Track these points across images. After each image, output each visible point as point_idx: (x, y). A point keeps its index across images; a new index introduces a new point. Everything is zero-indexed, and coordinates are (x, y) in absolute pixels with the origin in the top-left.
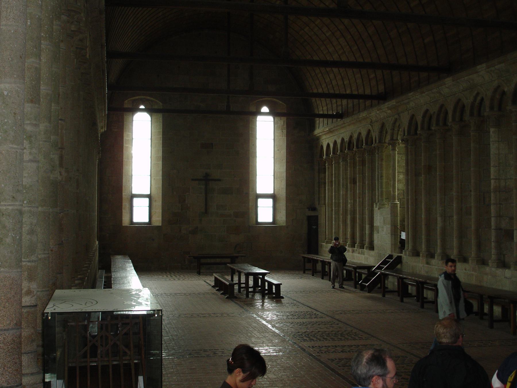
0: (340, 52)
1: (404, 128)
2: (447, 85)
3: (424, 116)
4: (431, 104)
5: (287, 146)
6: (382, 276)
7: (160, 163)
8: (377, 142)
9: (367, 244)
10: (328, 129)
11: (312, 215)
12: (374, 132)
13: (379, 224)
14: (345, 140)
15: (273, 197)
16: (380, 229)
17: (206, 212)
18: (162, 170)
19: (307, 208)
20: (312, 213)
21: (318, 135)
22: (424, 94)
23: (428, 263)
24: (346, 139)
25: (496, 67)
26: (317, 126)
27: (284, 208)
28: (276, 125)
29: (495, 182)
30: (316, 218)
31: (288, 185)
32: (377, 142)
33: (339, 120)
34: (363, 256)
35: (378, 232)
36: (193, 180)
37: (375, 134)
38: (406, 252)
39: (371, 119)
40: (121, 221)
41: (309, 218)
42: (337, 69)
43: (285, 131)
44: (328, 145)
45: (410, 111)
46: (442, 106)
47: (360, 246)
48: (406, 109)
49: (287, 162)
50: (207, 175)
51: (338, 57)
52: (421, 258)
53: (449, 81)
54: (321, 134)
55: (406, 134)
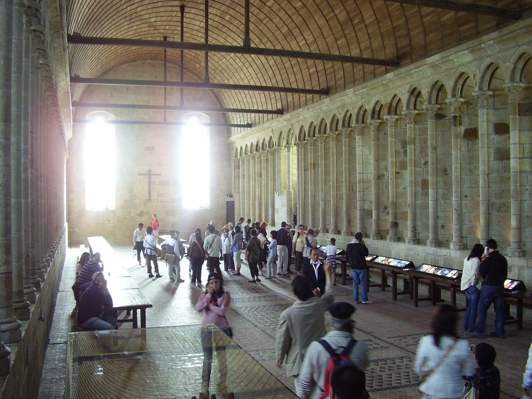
2: (326, 104)
3: (310, 127)
8: (277, 145)
14: (254, 144)
16: (279, 211)
17: (150, 199)
20: (230, 199)
21: (234, 140)
22: (309, 110)
24: (255, 144)
25: (360, 91)
26: (233, 133)
29: (360, 175)
32: (277, 145)
33: (249, 128)
35: (278, 213)
36: (139, 175)
37: (275, 140)
41: (228, 203)
42: (247, 91)
44: (241, 148)
46: (323, 119)
50: (150, 171)
53: (327, 101)
55: (297, 140)
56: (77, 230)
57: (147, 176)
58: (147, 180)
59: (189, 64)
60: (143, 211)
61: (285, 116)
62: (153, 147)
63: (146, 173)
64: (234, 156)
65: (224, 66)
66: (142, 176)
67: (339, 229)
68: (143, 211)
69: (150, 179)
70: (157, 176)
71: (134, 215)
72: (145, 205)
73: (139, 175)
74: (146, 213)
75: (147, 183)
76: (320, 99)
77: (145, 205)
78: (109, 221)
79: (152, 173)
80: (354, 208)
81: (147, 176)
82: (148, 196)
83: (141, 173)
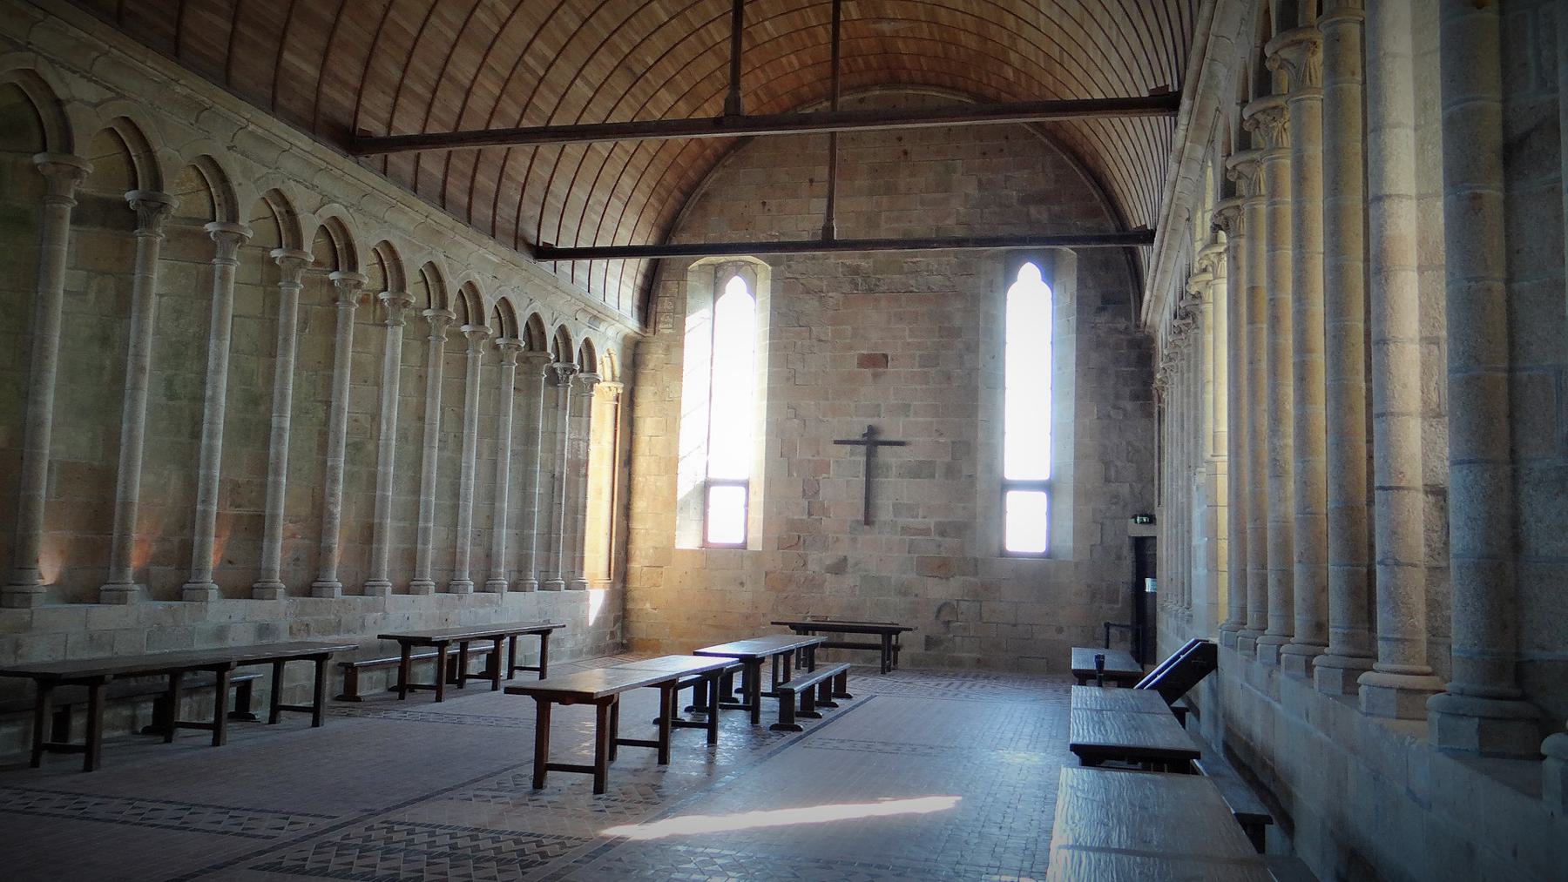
5: (1078, 358)
7: (764, 403)
15: (1049, 487)
17: (868, 520)
18: (767, 422)
19: (1133, 518)
20: (1144, 531)
27: (1071, 515)
28: (1055, 307)
31: (1079, 457)
36: (836, 442)
40: (671, 539)
42: (1154, 117)
43: (1073, 319)
49: (1079, 398)
57: (863, 448)
58: (863, 459)
60: (845, 559)
62: (886, 356)
63: (857, 438)
66: (848, 447)
68: (845, 559)
69: (870, 455)
70: (895, 448)
71: (817, 569)
72: (854, 540)
73: (836, 442)
74: (856, 564)
75: (862, 469)
77: (854, 540)
78: (742, 584)
79: (882, 438)
81: (863, 448)
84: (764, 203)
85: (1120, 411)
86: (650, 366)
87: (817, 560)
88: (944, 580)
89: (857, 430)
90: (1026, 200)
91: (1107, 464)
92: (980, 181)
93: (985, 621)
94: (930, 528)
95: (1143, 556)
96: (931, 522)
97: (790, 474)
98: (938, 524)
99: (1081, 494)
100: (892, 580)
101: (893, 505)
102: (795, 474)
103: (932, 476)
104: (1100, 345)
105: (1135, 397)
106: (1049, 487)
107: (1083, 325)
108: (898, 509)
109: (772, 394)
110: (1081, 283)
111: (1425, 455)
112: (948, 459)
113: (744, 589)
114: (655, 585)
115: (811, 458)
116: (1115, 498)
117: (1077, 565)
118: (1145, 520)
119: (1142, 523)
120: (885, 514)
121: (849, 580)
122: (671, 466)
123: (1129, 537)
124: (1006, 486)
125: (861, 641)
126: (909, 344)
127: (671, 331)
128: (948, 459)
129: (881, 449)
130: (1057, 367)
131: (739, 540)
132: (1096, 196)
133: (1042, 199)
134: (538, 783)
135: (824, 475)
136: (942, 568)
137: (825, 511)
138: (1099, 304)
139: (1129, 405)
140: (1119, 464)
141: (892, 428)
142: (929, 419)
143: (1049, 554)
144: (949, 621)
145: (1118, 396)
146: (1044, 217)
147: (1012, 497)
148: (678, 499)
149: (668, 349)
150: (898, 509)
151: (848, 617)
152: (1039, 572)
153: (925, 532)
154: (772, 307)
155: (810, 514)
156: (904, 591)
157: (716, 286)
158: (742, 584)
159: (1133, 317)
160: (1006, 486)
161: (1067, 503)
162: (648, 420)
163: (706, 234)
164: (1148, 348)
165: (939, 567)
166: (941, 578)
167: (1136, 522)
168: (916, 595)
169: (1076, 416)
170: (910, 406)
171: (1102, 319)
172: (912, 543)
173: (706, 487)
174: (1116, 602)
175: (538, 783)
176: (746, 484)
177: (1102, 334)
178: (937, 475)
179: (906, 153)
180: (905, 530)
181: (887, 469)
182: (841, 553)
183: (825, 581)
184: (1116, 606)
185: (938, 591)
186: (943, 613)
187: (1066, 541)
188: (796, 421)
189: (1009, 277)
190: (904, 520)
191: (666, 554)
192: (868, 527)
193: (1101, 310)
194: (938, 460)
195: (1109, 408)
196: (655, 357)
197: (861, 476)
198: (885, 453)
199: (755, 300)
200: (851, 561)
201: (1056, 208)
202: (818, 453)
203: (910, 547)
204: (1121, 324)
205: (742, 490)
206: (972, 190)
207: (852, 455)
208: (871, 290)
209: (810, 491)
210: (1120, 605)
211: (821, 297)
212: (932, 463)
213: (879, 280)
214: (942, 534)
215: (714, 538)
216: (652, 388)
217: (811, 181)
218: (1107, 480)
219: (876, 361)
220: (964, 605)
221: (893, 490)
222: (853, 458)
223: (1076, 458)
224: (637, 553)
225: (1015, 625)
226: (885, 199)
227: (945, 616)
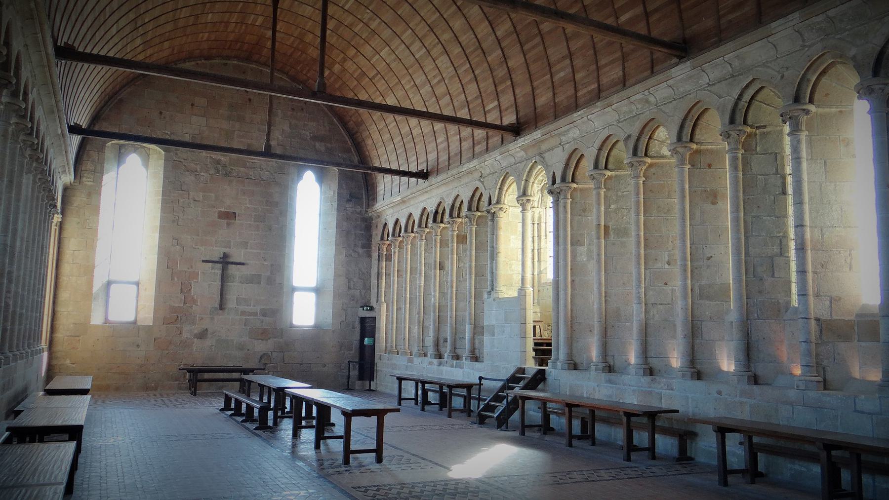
0: (434, 82)
1: (554, 173)
2: (671, 82)
4: (619, 125)
6: (520, 401)
7: (157, 235)
9: (465, 353)
10: (400, 198)
11: (367, 316)
12: (486, 189)
13: (494, 322)
15: (318, 291)
17: (222, 307)
19: (361, 307)
23: (610, 381)
28: (322, 197)
30: (374, 318)
31: (336, 275)
34: (461, 371)
36: (204, 261)
38: (554, 363)
39: (481, 172)
40: (88, 318)
41: (363, 320)
43: (335, 204)
45: (567, 146)
47: (452, 356)
48: (560, 144)
49: (337, 245)
50: (225, 256)
51: (431, 89)
52: (593, 373)
54: (384, 208)
56: (68, 362)
57: (220, 265)
58: (219, 272)
59: (308, 71)
61: (528, 137)
62: (235, 213)
63: (216, 259)
64: (379, 237)
65: (381, 67)
66: (210, 264)
67: (698, 367)
69: (224, 270)
72: (212, 319)
73: (204, 261)
75: (219, 277)
76: (652, 72)
78: (138, 346)
79: (231, 260)
80: (758, 318)
82: (218, 301)
83: (207, 259)
84: (161, 113)
85: (357, 253)
86: (75, 205)
87: (188, 331)
88: (264, 341)
89: (217, 253)
90: (315, 138)
91: (349, 280)
92: (290, 124)
93: (286, 362)
94: (257, 312)
95: (367, 327)
96: (258, 309)
97: (173, 279)
98: (261, 310)
99: (337, 295)
100: (235, 342)
101: (237, 299)
102: (176, 279)
103: (259, 283)
104: (348, 219)
105: (363, 247)
106: (317, 290)
107: (340, 208)
108: (239, 301)
109: (163, 229)
110: (340, 186)
111: (814, 307)
112: (268, 274)
113: (139, 349)
114: (73, 348)
115: (186, 269)
116: (353, 298)
117: (333, 331)
118: (368, 308)
119: (367, 310)
120: (231, 304)
121: (209, 342)
122: (89, 271)
123: (359, 317)
124: (294, 289)
125: (215, 377)
126: (248, 208)
127: (92, 183)
128: (268, 274)
129: (231, 267)
130: (324, 228)
131: (131, 318)
132: (349, 142)
133: (321, 139)
134: (346, 461)
135: (194, 280)
136: (264, 334)
137: (194, 301)
138: (348, 197)
139: (361, 251)
140: (355, 280)
141: (237, 255)
142: (259, 251)
143: (316, 326)
144: (266, 364)
145: (355, 246)
146: (323, 149)
147: (297, 296)
148: (93, 292)
149: (89, 195)
150: (239, 301)
151: (208, 364)
152: (316, 334)
153: (255, 314)
154: (165, 177)
155: (185, 303)
156: (241, 347)
157: (120, 158)
158: (138, 346)
159: (364, 207)
160: (294, 289)
161: (329, 299)
162: (73, 240)
163: (119, 125)
164: (371, 223)
165: (262, 334)
166: (262, 340)
167: (364, 310)
168: (248, 350)
169: (336, 255)
170: (248, 243)
171: (349, 206)
172: (246, 320)
173: (109, 284)
174: (352, 350)
175: (346, 461)
176: (137, 284)
177: (350, 214)
178: (262, 283)
179: (250, 100)
180: (243, 313)
181: (233, 277)
182: (204, 327)
183: (193, 343)
184: (351, 352)
185: (261, 347)
186: (263, 359)
187: (328, 318)
188: (178, 247)
189: (300, 177)
190: (242, 308)
191: (84, 326)
192: (221, 311)
193: (349, 201)
194: (263, 274)
195: (351, 251)
196: (79, 199)
197: (218, 281)
198: (232, 269)
199: (147, 170)
200: (210, 331)
201: (329, 145)
202: (192, 267)
203: (245, 323)
204: (358, 209)
205: (135, 287)
206: (286, 128)
207: (212, 268)
208: (226, 175)
209: (185, 289)
210: (353, 352)
211: (196, 175)
212: (260, 276)
213: (232, 169)
214: (264, 315)
215: (113, 317)
216: (76, 219)
217: (192, 105)
218: (349, 288)
219: (229, 216)
220: (275, 354)
221: (236, 290)
222: (213, 271)
223: (335, 276)
224: (61, 327)
225: (301, 364)
226: (237, 125)
227: (263, 361)
